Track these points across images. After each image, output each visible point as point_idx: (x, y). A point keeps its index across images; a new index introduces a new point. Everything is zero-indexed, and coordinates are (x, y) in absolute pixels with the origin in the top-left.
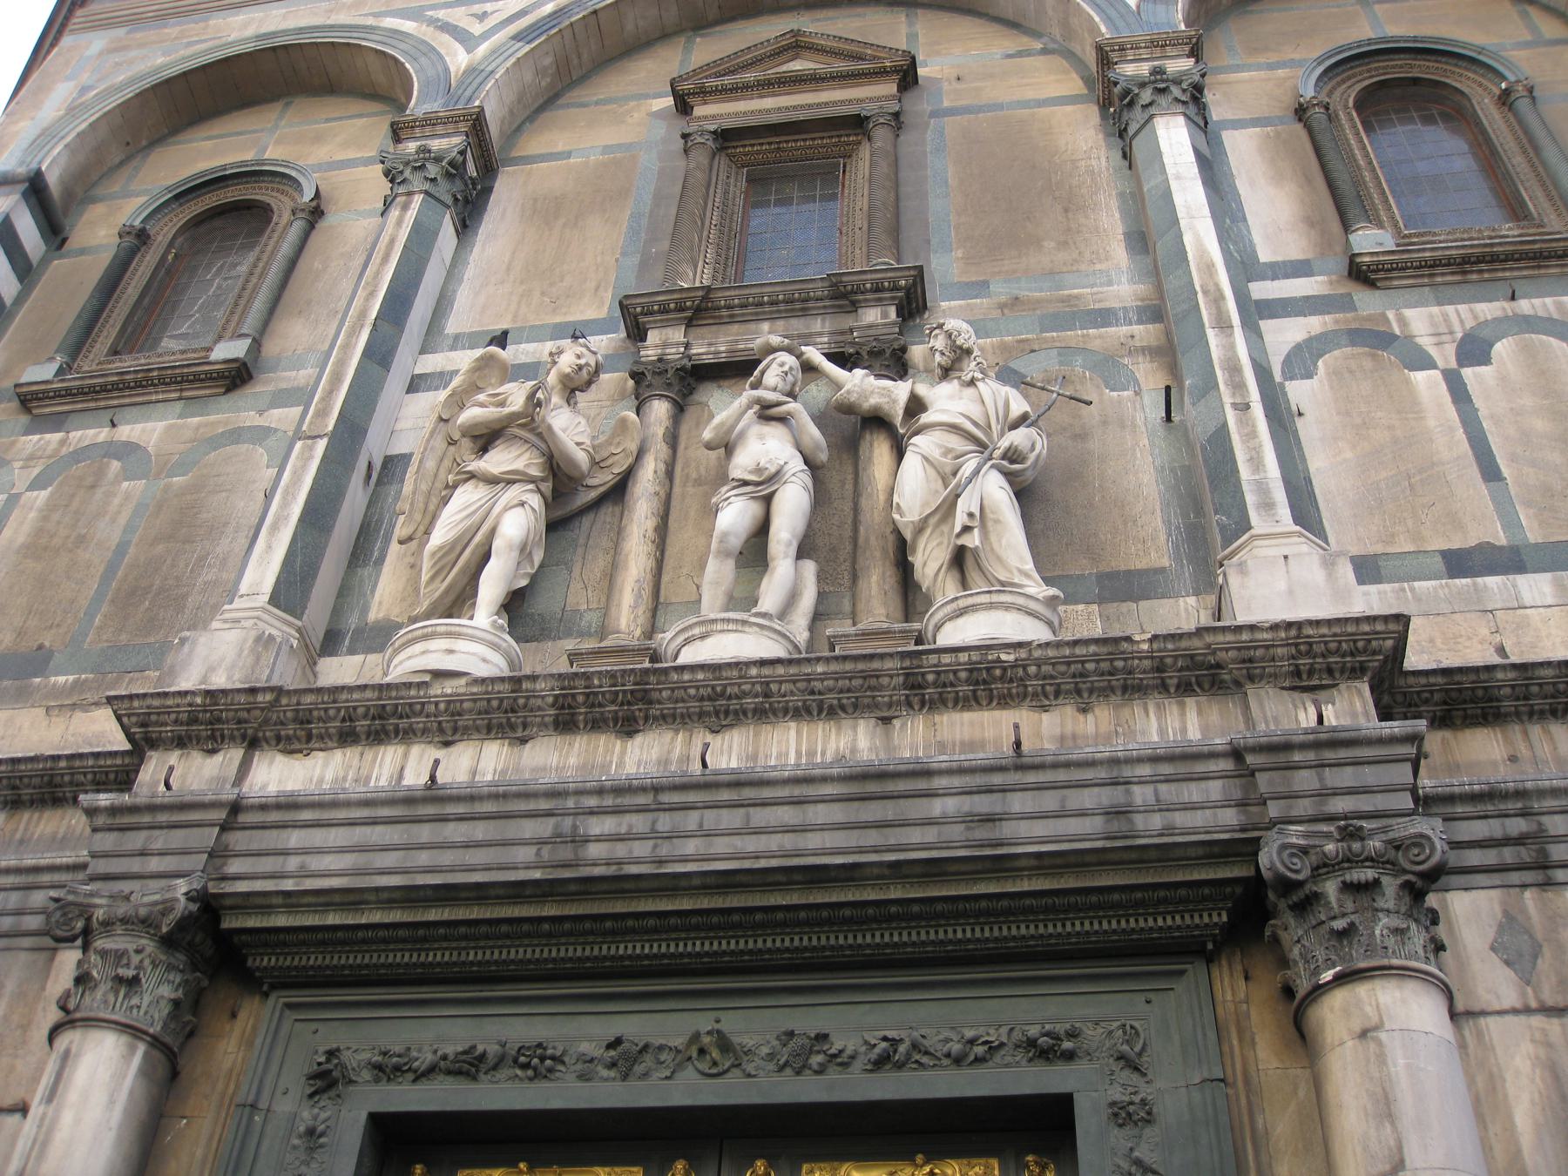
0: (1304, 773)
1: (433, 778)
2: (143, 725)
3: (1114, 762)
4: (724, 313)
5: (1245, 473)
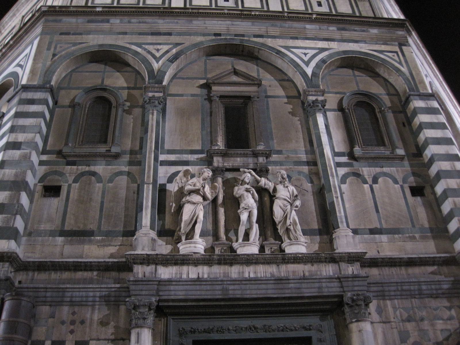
0: (350, 282)
1: (199, 277)
2: (133, 260)
3: (320, 279)
4: (230, 155)
5: (338, 214)
